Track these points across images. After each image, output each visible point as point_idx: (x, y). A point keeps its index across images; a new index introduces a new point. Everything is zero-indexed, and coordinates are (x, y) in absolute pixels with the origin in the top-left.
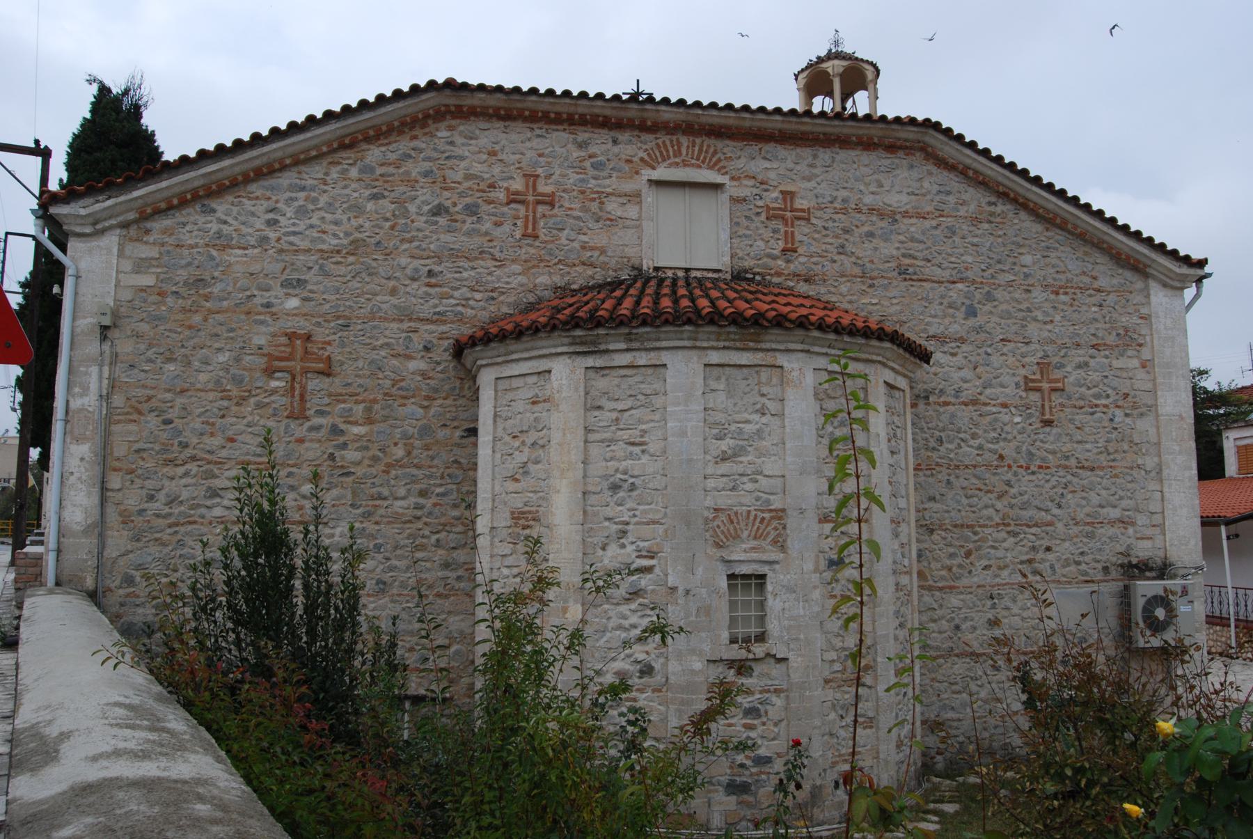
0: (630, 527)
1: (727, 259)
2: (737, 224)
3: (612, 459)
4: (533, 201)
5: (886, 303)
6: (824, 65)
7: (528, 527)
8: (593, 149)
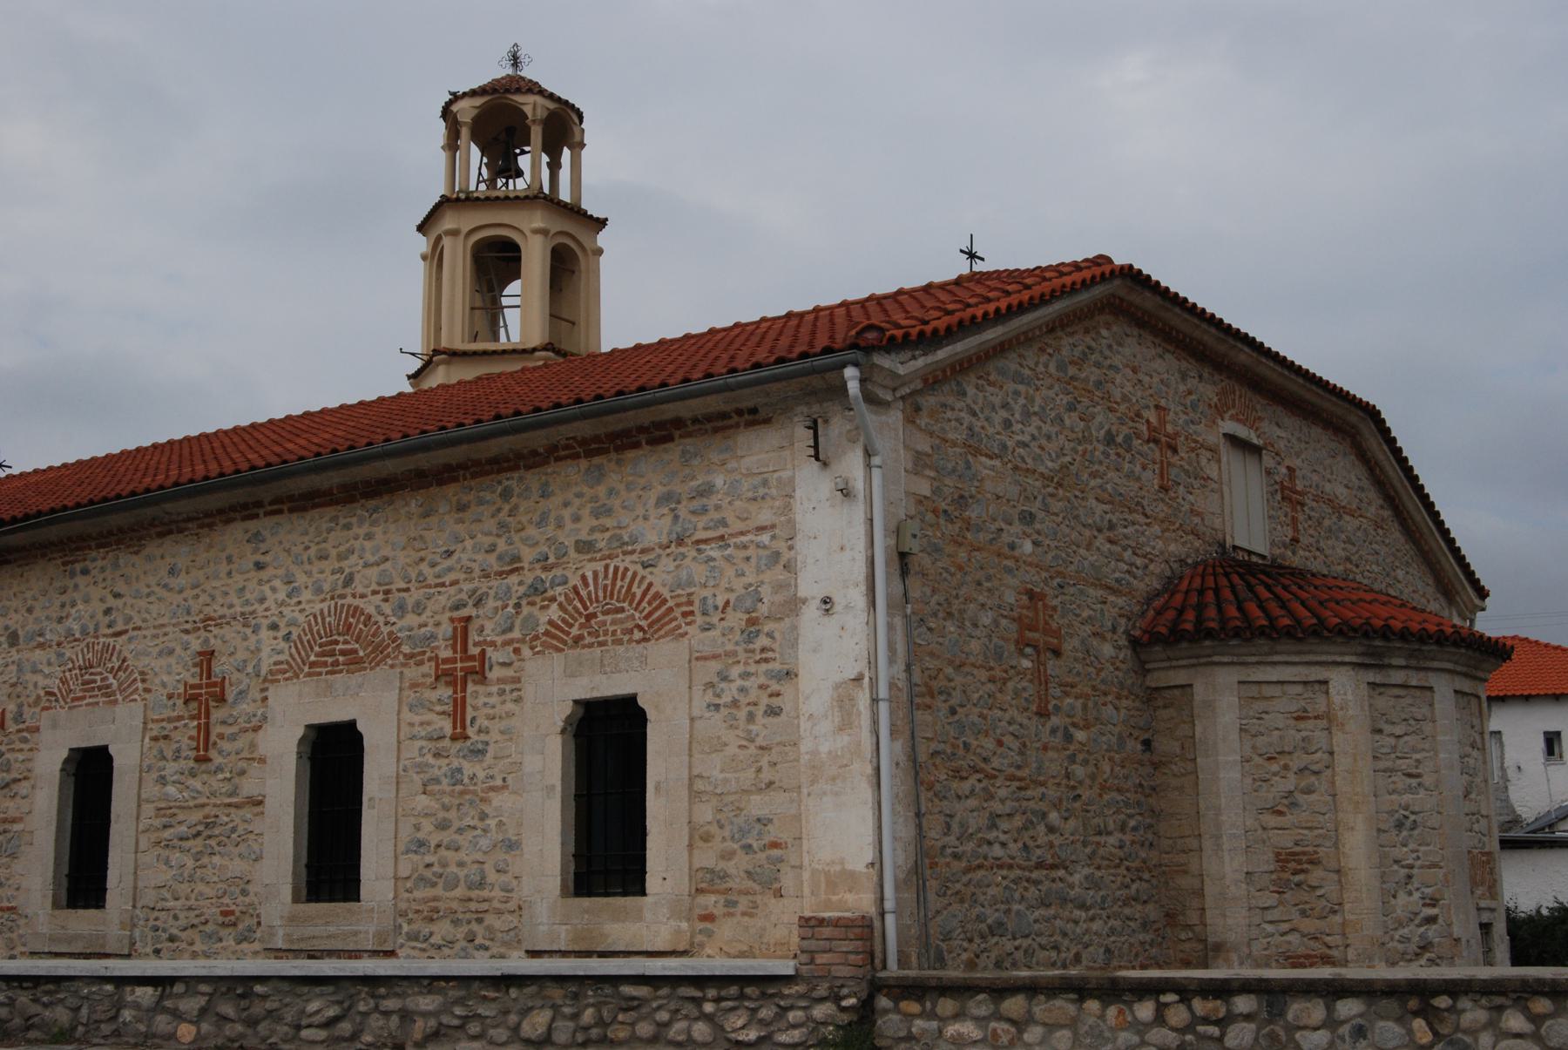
0: (1415, 871)
3: (1394, 791)
7: (1303, 871)
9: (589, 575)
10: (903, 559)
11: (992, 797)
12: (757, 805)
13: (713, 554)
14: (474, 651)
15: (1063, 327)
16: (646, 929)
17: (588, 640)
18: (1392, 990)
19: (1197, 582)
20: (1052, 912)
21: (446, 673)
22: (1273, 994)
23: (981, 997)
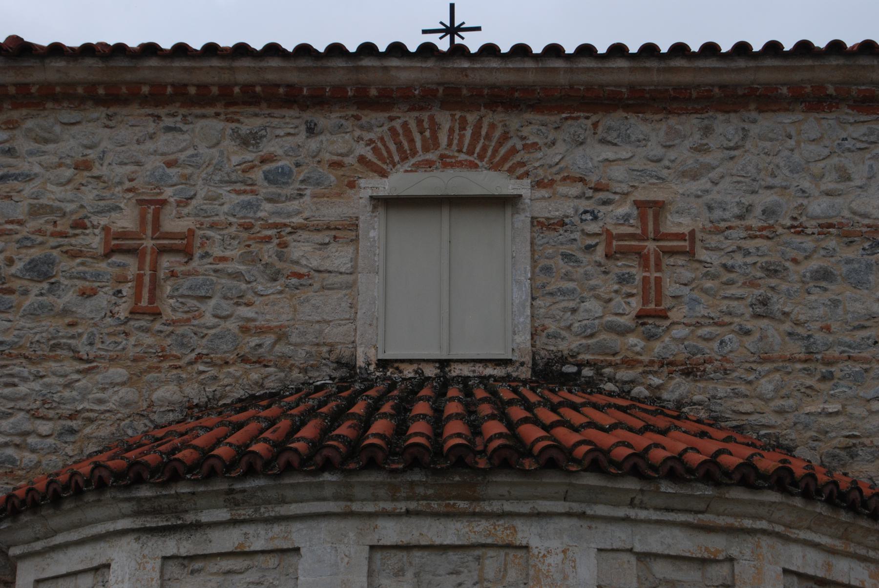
1: (523, 339)
2: (547, 270)
4: (153, 248)
5: (858, 411)
8: (269, 147)
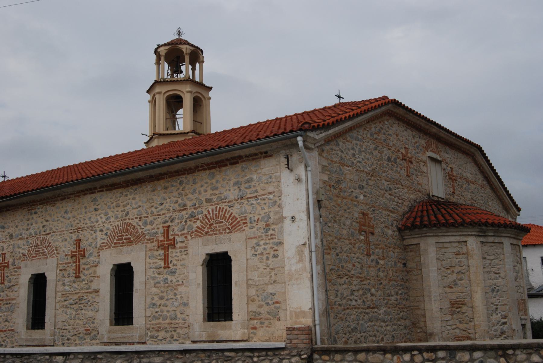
0: (499, 306)
3: (491, 279)
6: (181, 46)
7: (460, 307)
9: (211, 210)
10: (319, 203)
11: (351, 284)
12: (270, 289)
13: (253, 202)
14: (171, 237)
15: (372, 121)
16: (234, 332)
17: (210, 233)
18: (493, 348)
19: (420, 209)
20: (373, 323)
21: (161, 245)
22: (451, 350)
23: (350, 353)
